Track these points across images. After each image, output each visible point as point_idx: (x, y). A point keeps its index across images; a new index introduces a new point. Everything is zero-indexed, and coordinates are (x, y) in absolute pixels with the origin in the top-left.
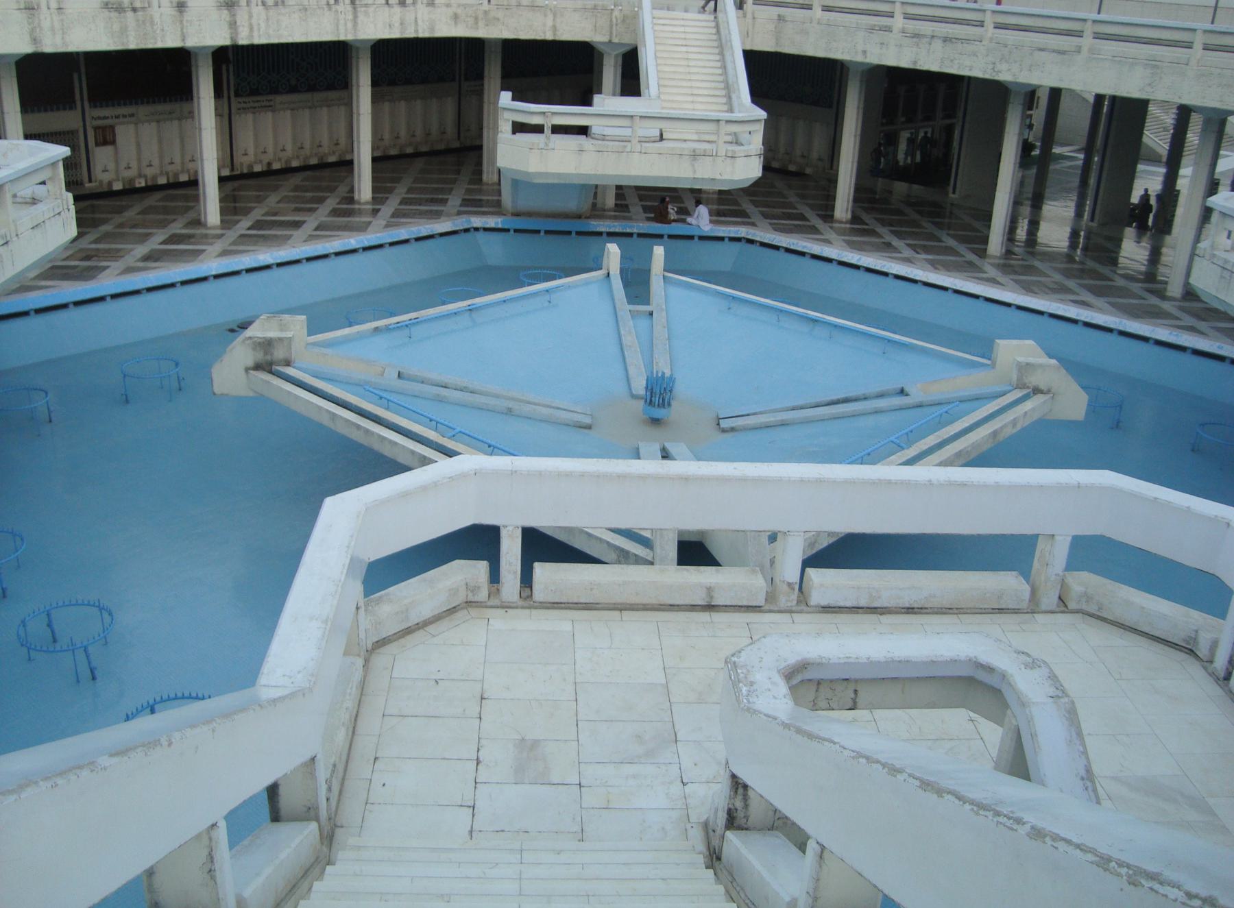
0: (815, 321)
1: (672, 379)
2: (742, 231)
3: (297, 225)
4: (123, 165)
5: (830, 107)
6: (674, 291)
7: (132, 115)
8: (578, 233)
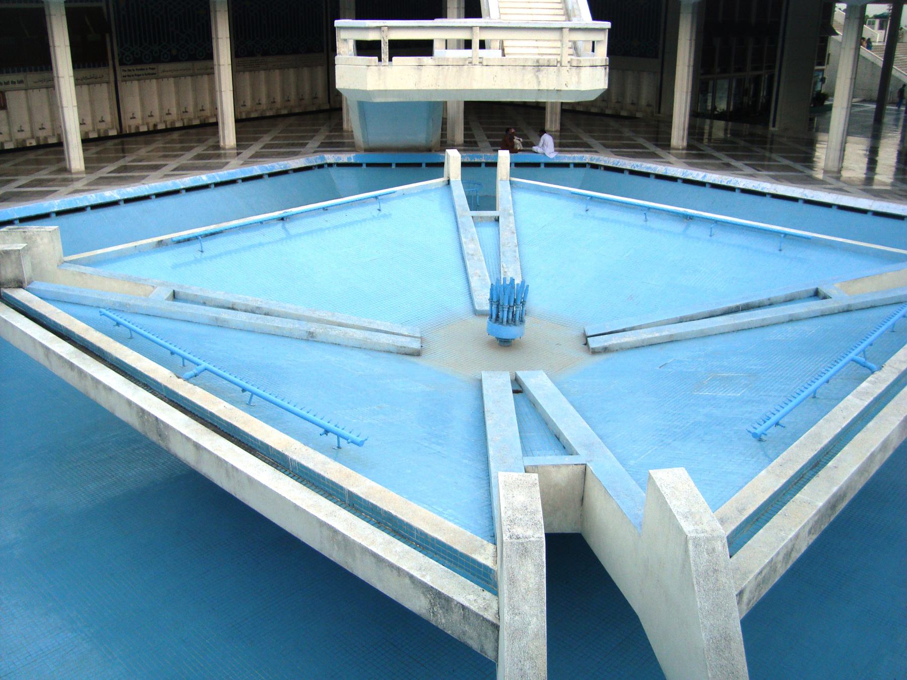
0: (690, 218)
1: (524, 288)
2: (587, 158)
3: (156, 168)
4: (16, 129)
5: (656, 57)
6: (524, 198)
7: (21, 82)
8: (428, 165)
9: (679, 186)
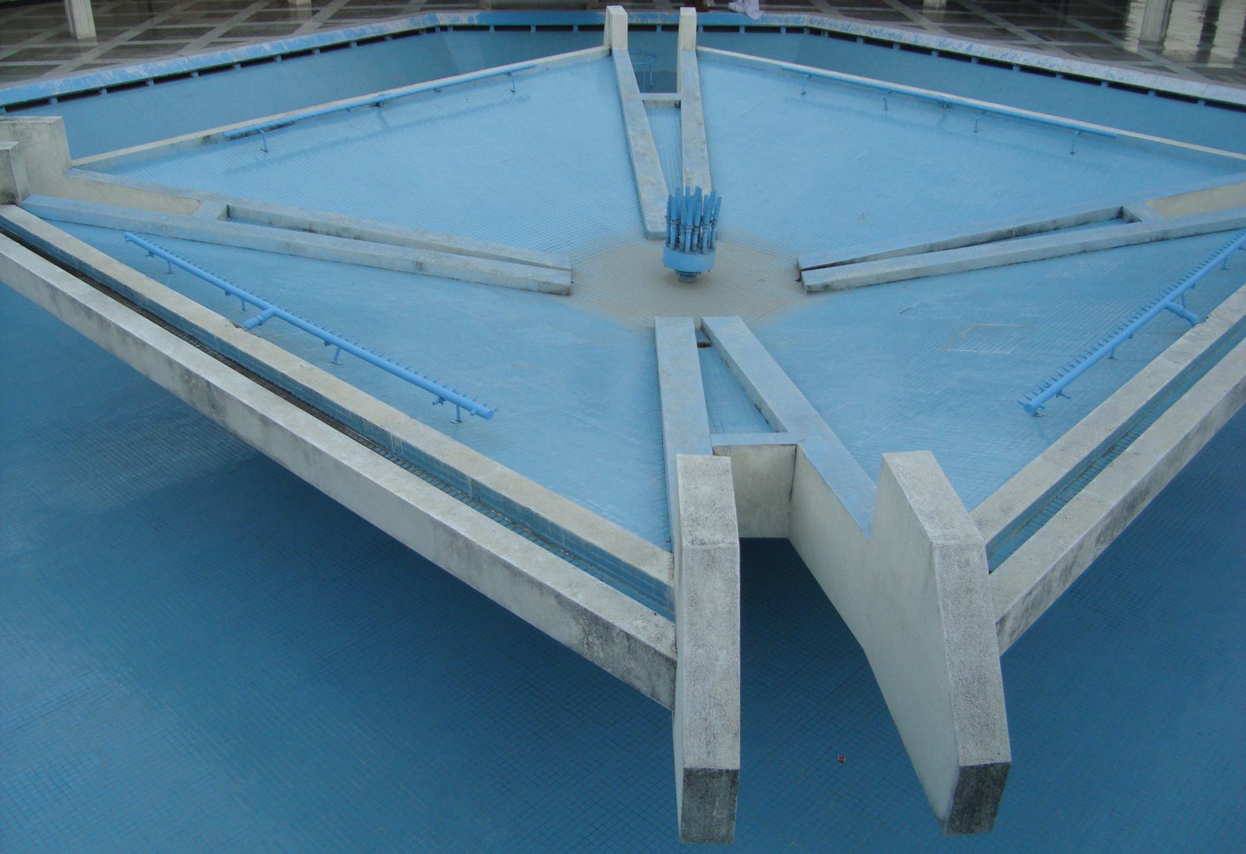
0: (946, 106)
1: (714, 202)
6: (715, 74)
8: (582, 28)
9: (934, 60)
